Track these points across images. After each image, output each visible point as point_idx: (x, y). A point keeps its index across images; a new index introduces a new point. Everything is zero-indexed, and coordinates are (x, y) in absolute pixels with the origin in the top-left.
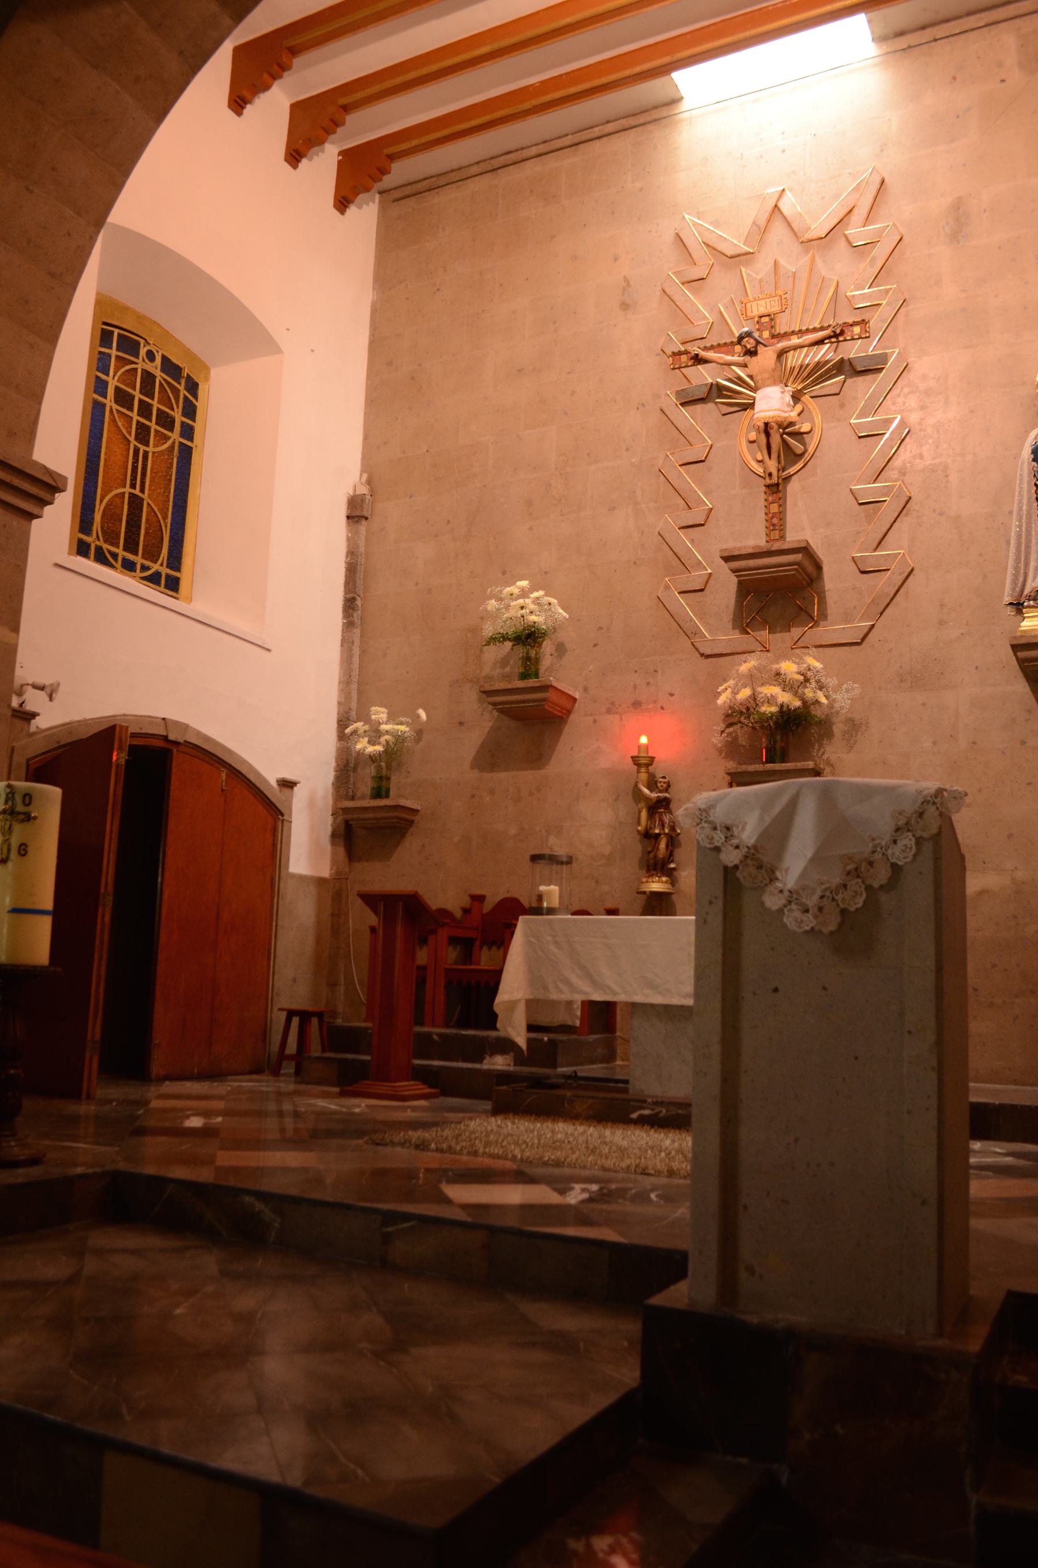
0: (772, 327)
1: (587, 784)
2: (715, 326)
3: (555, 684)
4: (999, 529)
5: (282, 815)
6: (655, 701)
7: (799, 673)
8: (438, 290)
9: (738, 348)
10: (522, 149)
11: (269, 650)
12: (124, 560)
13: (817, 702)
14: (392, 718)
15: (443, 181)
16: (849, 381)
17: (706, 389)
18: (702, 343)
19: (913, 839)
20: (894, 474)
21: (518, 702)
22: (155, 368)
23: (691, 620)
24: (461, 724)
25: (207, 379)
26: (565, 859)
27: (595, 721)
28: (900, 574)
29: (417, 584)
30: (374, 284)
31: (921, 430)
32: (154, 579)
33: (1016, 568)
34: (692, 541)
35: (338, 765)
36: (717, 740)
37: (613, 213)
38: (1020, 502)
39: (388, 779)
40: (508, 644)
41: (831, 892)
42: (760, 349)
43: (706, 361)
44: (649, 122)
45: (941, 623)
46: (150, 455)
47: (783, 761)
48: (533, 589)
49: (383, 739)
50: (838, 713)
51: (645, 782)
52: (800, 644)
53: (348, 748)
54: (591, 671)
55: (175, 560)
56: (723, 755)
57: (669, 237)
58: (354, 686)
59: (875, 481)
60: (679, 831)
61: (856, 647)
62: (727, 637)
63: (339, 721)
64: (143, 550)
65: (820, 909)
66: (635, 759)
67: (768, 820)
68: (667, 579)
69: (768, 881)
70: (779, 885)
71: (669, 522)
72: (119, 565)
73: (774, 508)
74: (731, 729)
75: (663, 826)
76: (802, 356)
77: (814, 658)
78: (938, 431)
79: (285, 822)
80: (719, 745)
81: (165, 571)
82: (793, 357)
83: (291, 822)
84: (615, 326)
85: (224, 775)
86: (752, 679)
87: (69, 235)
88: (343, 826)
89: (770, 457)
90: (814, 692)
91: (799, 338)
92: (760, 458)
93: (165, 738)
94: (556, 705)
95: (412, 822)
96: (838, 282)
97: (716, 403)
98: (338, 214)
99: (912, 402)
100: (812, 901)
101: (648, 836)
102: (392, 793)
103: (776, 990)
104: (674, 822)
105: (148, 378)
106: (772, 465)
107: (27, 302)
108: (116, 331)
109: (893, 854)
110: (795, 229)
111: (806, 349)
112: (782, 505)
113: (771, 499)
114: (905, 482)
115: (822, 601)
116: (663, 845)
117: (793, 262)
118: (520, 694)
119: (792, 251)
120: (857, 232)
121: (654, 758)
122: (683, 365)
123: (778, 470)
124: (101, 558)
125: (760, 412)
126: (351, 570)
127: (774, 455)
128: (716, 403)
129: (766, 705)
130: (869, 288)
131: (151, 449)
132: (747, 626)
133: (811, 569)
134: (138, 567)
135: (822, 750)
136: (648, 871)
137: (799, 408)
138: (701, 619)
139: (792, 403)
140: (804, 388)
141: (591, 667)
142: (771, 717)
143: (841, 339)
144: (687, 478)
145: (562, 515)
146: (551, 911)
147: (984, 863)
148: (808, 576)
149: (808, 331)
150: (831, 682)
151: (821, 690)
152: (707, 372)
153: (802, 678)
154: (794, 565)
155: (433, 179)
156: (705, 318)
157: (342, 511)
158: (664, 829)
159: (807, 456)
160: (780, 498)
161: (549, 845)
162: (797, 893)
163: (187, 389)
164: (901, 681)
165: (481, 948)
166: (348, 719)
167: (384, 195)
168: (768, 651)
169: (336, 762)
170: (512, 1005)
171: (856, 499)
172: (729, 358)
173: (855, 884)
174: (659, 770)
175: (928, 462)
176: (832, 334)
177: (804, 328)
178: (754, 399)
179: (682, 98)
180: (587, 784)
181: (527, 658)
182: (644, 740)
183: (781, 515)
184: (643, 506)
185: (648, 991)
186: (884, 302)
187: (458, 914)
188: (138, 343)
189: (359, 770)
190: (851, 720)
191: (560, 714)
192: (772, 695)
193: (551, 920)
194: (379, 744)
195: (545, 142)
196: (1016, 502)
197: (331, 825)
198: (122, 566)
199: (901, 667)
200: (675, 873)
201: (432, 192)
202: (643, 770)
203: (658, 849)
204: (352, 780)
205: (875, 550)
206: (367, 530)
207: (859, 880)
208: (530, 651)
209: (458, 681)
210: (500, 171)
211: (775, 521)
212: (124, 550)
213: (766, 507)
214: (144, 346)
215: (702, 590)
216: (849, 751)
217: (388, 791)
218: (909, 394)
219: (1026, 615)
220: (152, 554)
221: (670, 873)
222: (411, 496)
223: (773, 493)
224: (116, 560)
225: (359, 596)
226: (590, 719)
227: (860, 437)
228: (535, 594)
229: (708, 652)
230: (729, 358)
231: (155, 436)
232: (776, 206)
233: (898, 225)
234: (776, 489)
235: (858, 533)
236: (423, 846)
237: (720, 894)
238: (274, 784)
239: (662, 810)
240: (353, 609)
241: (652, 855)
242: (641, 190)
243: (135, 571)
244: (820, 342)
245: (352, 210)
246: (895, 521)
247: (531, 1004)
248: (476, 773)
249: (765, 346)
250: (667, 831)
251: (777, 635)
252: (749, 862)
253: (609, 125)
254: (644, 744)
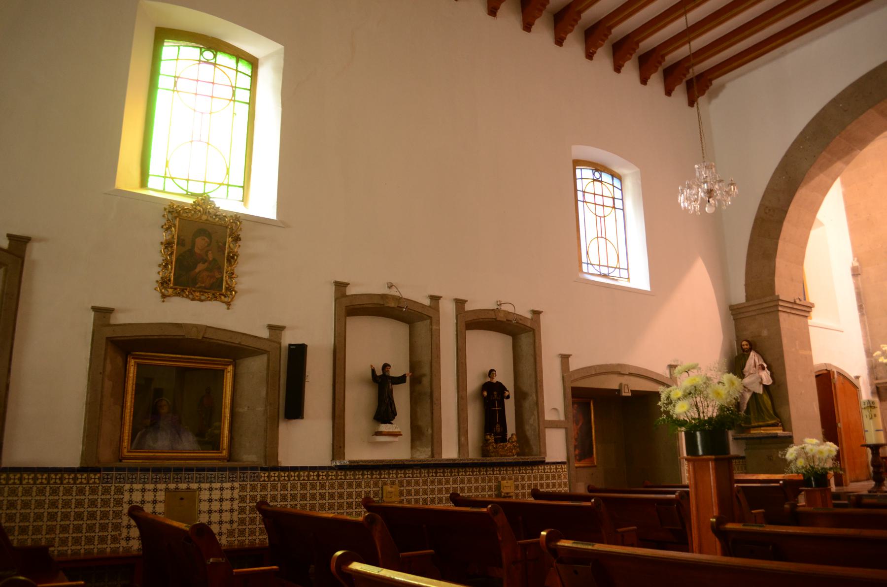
11: (843, 332)
35: (869, 367)
58: (869, 337)
88: (875, 389)
93: (827, 370)
126: (859, 295)
157: (850, 273)
238: (853, 378)
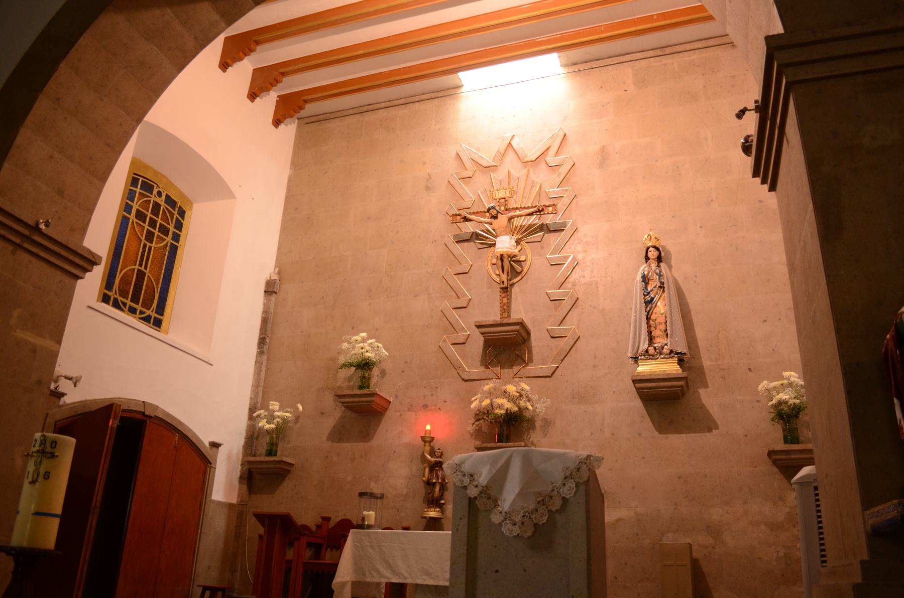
0: (506, 205)
1: (395, 452)
2: (476, 201)
3: (378, 393)
4: (625, 317)
5: (211, 464)
6: (435, 405)
7: (517, 392)
8: (326, 172)
9: (487, 214)
10: (377, 103)
11: (212, 365)
12: (130, 307)
13: (527, 408)
14: (281, 408)
15: (332, 116)
16: (546, 235)
17: (470, 235)
18: (468, 211)
19: (574, 483)
20: (570, 285)
22: (161, 201)
23: (458, 360)
24: (322, 413)
25: (191, 209)
26: (379, 496)
27: (401, 415)
28: (573, 339)
29: (302, 332)
30: (291, 166)
31: (584, 263)
32: (147, 319)
33: (634, 338)
34: (459, 316)
35: (247, 435)
36: (471, 428)
37: (424, 140)
38: (636, 303)
39: (277, 444)
40: (353, 369)
41: (529, 513)
42: (499, 215)
43: (470, 220)
44: (446, 96)
45: (595, 366)
46: (153, 248)
47: (507, 442)
48: (369, 338)
49: (275, 421)
50: (538, 415)
51: (428, 452)
52: (518, 375)
53: (254, 425)
54: (400, 386)
55: (161, 309)
56: (474, 437)
57: (453, 154)
58: (261, 389)
59: (559, 289)
60: (447, 481)
61: (548, 379)
62: (478, 370)
63: (250, 409)
64: (142, 302)
65: (523, 523)
66: (423, 439)
67: (494, 471)
68: (445, 336)
69: (493, 506)
70: (500, 509)
71: (447, 305)
72: (126, 310)
73: (505, 300)
74: (478, 423)
75: (438, 478)
76: (522, 221)
77: (525, 383)
78: (593, 264)
79: (212, 469)
80: (472, 431)
81: (154, 315)
82: (517, 220)
83: (216, 468)
84: (422, 198)
85: (177, 438)
86: (490, 394)
87: (121, 125)
88: (247, 472)
89: (503, 273)
90: (525, 403)
91: (520, 211)
92: (498, 273)
93: (143, 413)
94: (379, 405)
95: (289, 471)
96: (541, 184)
97: (475, 243)
98: (274, 128)
99: (579, 248)
100: (518, 519)
101: (429, 484)
102: (279, 453)
103: (497, 571)
104: (444, 476)
105: (157, 206)
106: (504, 277)
107: (91, 158)
108: (141, 179)
109: (563, 492)
110: (520, 155)
111: (524, 217)
112: (509, 299)
113: (503, 295)
114: (575, 289)
115: (530, 352)
116: (437, 489)
117: (518, 172)
119: (517, 167)
120: (551, 159)
121: (434, 438)
122: (458, 221)
123: (508, 280)
124: (116, 305)
125: (498, 248)
126: (265, 321)
127: (505, 272)
128: (475, 243)
129: (498, 409)
130: (557, 188)
131: (153, 245)
132: (489, 364)
133: (524, 334)
134: (138, 311)
135: (529, 436)
136: (428, 505)
137: (519, 247)
138: (463, 359)
139: (515, 245)
140: (522, 237)
141: (400, 384)
142: (501, 416)
143: (542, 213)
144: (458, 281)
145: (388, 298)
146: (369, 527)
147: (620, 503)
148: (522, 338)
149: (525, 208)
150: (535, 397)
151: (529, 402)
152: (471, 226)
153: (518, 395)
154: (515, 332)
155: (328, 115)
156: (471, 198)
157: (262, 288)
158: (438, 480)
159: (523, 274)
160: (508, 295)
162: (510, 513)
163: (178, 214)
164: (573, 398)
165: (326, 550)
166: (255, 408)
167: (300, 120)
168: (500, 379)
169: (246, 433)
170: (343, 584)
171: (549, 297)
172: (482, 219)
173: (542, 509)
174: (436, 445)
175: (587, 279)
176: (537, 210)
177: (523, 206)
178: (495, 241)
179: (463, 85)
180: (395, 452)
181: (363, 377)
182: (428, 427)
183: (509, 304)
184: (433, 295)
185: (425, 577)
186: (565, 196)
187: (314, 528)
188: (153, 186)
189: (260, 438)
190: (545, 420)
191: (381, 410)
192: (501, 404)
193: (369, 533)
194: (273, 423)
195: (389, 101)
196: (634, 303)
197: (240, 471)
198: (128, 311)
199: (573, 390)
200: (444, 506)
201: (327, 121)
202: (427, 444)
203: (434, 492)
204: (255, 444)
205: (559, 326)
206: (276, 300)
207: (545, 507)
208: (365, 373)
209: (322, 389)
210: (364, 113)
211: (505, 307)
212: (131, 301)
213: (500, 299)
214: (156, 188)
215: (464, 343)
216: (544, 437)
217: (276, 451)
218: (577, 244)
219: (640, 364)
220: (147, 305)
221: (441, 506)
222: (302, 282)
223: (504, 292)
224: (125, 307)
225: (268, 336)
226: (398, 414)
227: (552, 265)
228: (370, 341)
229: (467, 378)
230: (482, 219)
231: (157, 238)
232: (510, 143)
233: (572, 157)
234: (506, 290)
235: (550, 316)
236: (295, 486)
237: (466, 514)
238: (207, 444)
239: (438, 468)
240: (264, 344)
241: (431, 495)
242: (439, 130)
243: (136, 314)
244: (531, 214)
245: (282, 127)
246: (570, 311)
247: (355, 584)
248: (329, 443)
249: (502, 214)
250: (440, 481)
251: (505, 370)
252: (483, 495)
253: (424, 95)
254: (428, 430)
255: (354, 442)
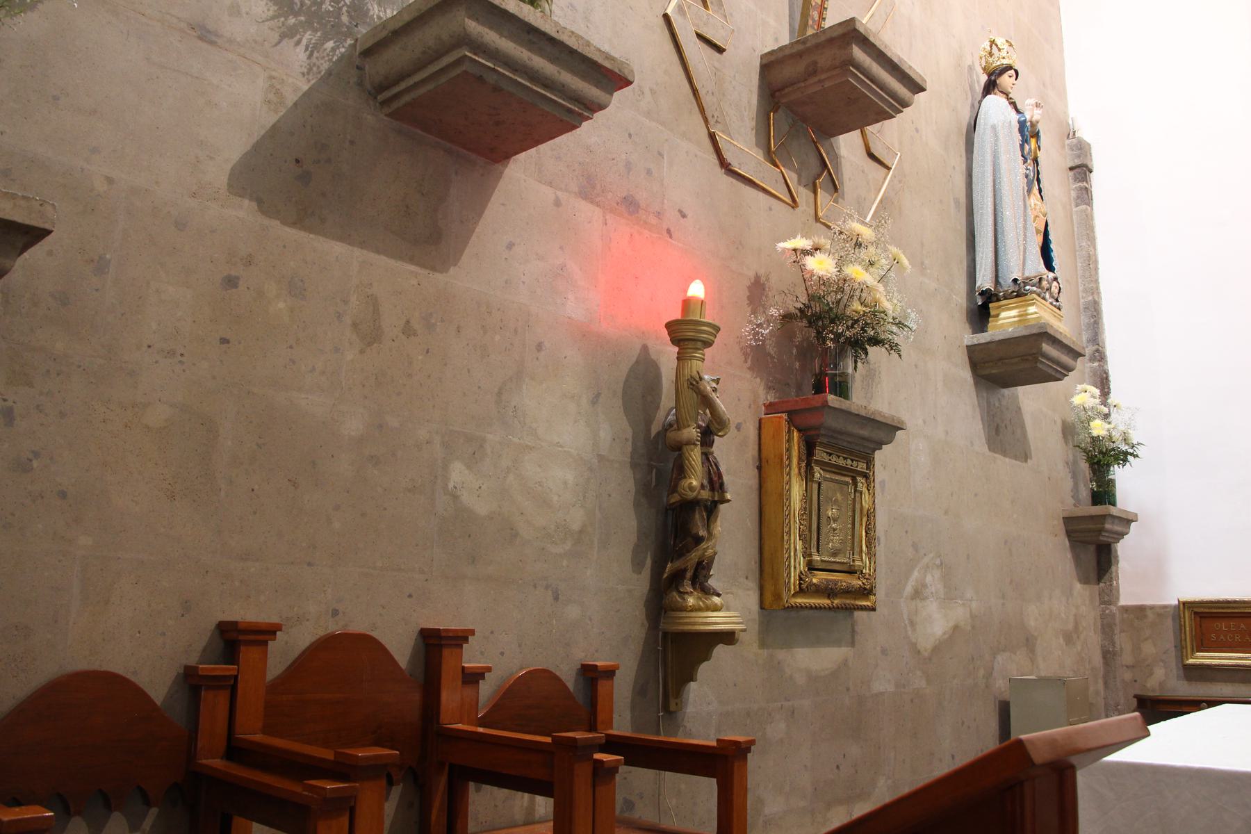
21: (534, 76)
118: (553, 60)
161: (451, 486)
182: (697, 290)
248: (244, 211)
255: (378, 252)
